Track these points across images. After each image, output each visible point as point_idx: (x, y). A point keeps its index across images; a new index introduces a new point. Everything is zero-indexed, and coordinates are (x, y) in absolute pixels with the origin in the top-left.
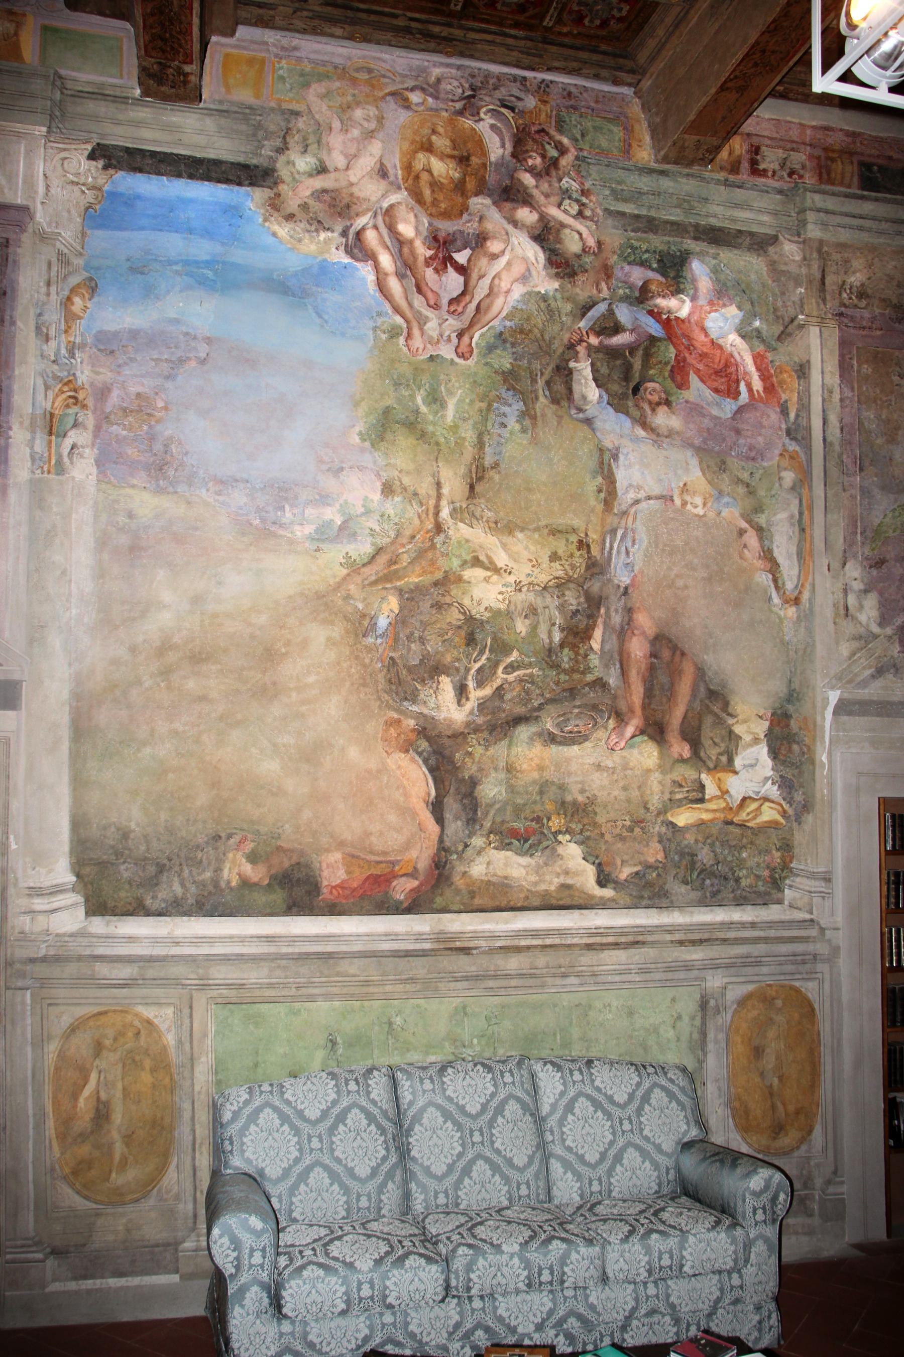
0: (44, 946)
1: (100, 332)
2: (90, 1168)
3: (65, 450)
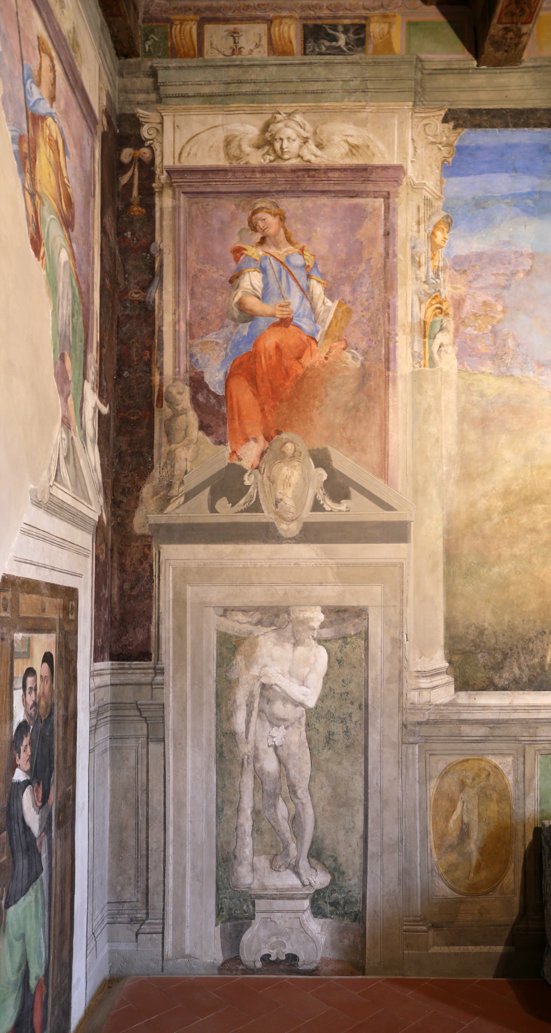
0: (427, 713)
1: (455, 257)
2: (456, 870)
3: (435, 348)
